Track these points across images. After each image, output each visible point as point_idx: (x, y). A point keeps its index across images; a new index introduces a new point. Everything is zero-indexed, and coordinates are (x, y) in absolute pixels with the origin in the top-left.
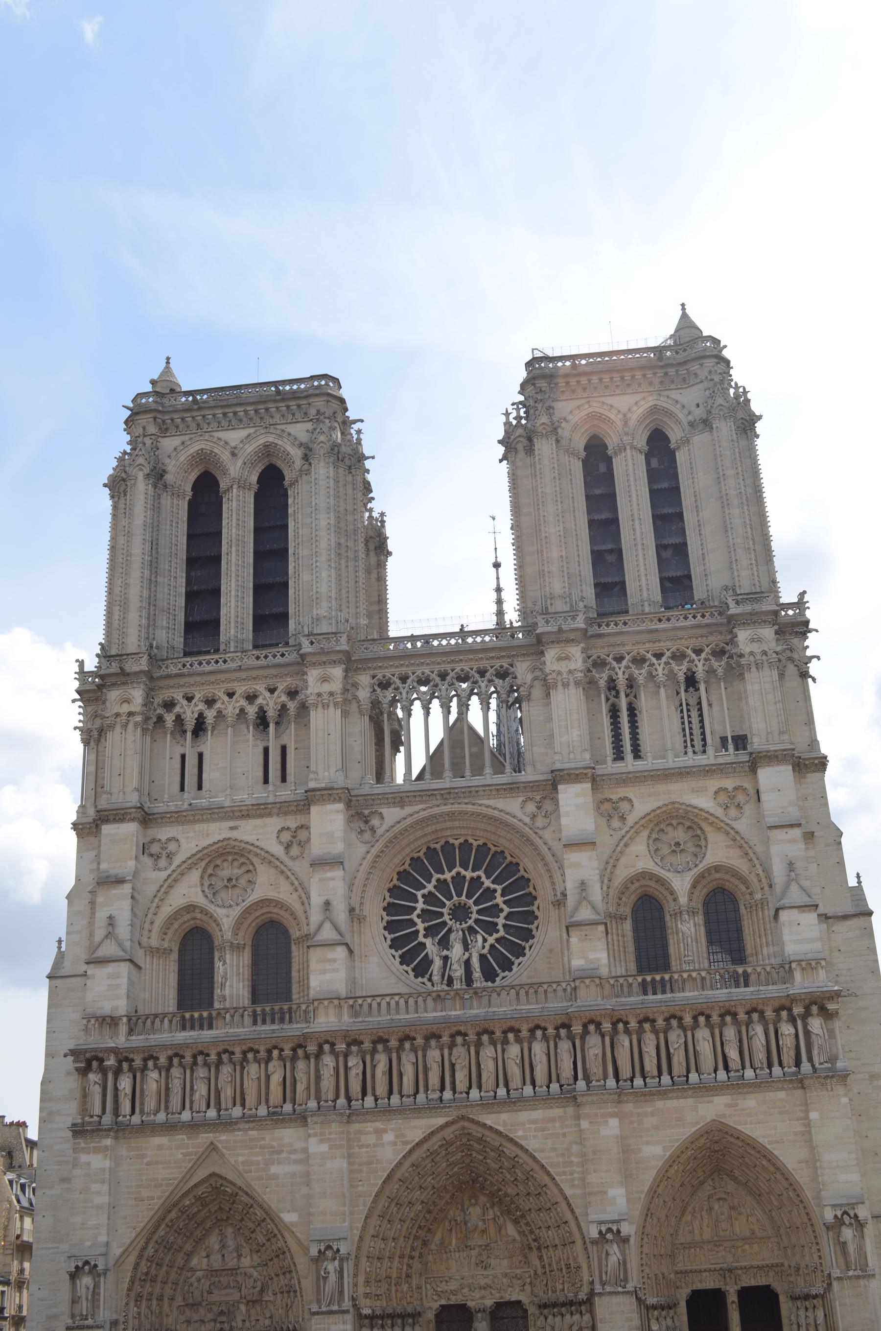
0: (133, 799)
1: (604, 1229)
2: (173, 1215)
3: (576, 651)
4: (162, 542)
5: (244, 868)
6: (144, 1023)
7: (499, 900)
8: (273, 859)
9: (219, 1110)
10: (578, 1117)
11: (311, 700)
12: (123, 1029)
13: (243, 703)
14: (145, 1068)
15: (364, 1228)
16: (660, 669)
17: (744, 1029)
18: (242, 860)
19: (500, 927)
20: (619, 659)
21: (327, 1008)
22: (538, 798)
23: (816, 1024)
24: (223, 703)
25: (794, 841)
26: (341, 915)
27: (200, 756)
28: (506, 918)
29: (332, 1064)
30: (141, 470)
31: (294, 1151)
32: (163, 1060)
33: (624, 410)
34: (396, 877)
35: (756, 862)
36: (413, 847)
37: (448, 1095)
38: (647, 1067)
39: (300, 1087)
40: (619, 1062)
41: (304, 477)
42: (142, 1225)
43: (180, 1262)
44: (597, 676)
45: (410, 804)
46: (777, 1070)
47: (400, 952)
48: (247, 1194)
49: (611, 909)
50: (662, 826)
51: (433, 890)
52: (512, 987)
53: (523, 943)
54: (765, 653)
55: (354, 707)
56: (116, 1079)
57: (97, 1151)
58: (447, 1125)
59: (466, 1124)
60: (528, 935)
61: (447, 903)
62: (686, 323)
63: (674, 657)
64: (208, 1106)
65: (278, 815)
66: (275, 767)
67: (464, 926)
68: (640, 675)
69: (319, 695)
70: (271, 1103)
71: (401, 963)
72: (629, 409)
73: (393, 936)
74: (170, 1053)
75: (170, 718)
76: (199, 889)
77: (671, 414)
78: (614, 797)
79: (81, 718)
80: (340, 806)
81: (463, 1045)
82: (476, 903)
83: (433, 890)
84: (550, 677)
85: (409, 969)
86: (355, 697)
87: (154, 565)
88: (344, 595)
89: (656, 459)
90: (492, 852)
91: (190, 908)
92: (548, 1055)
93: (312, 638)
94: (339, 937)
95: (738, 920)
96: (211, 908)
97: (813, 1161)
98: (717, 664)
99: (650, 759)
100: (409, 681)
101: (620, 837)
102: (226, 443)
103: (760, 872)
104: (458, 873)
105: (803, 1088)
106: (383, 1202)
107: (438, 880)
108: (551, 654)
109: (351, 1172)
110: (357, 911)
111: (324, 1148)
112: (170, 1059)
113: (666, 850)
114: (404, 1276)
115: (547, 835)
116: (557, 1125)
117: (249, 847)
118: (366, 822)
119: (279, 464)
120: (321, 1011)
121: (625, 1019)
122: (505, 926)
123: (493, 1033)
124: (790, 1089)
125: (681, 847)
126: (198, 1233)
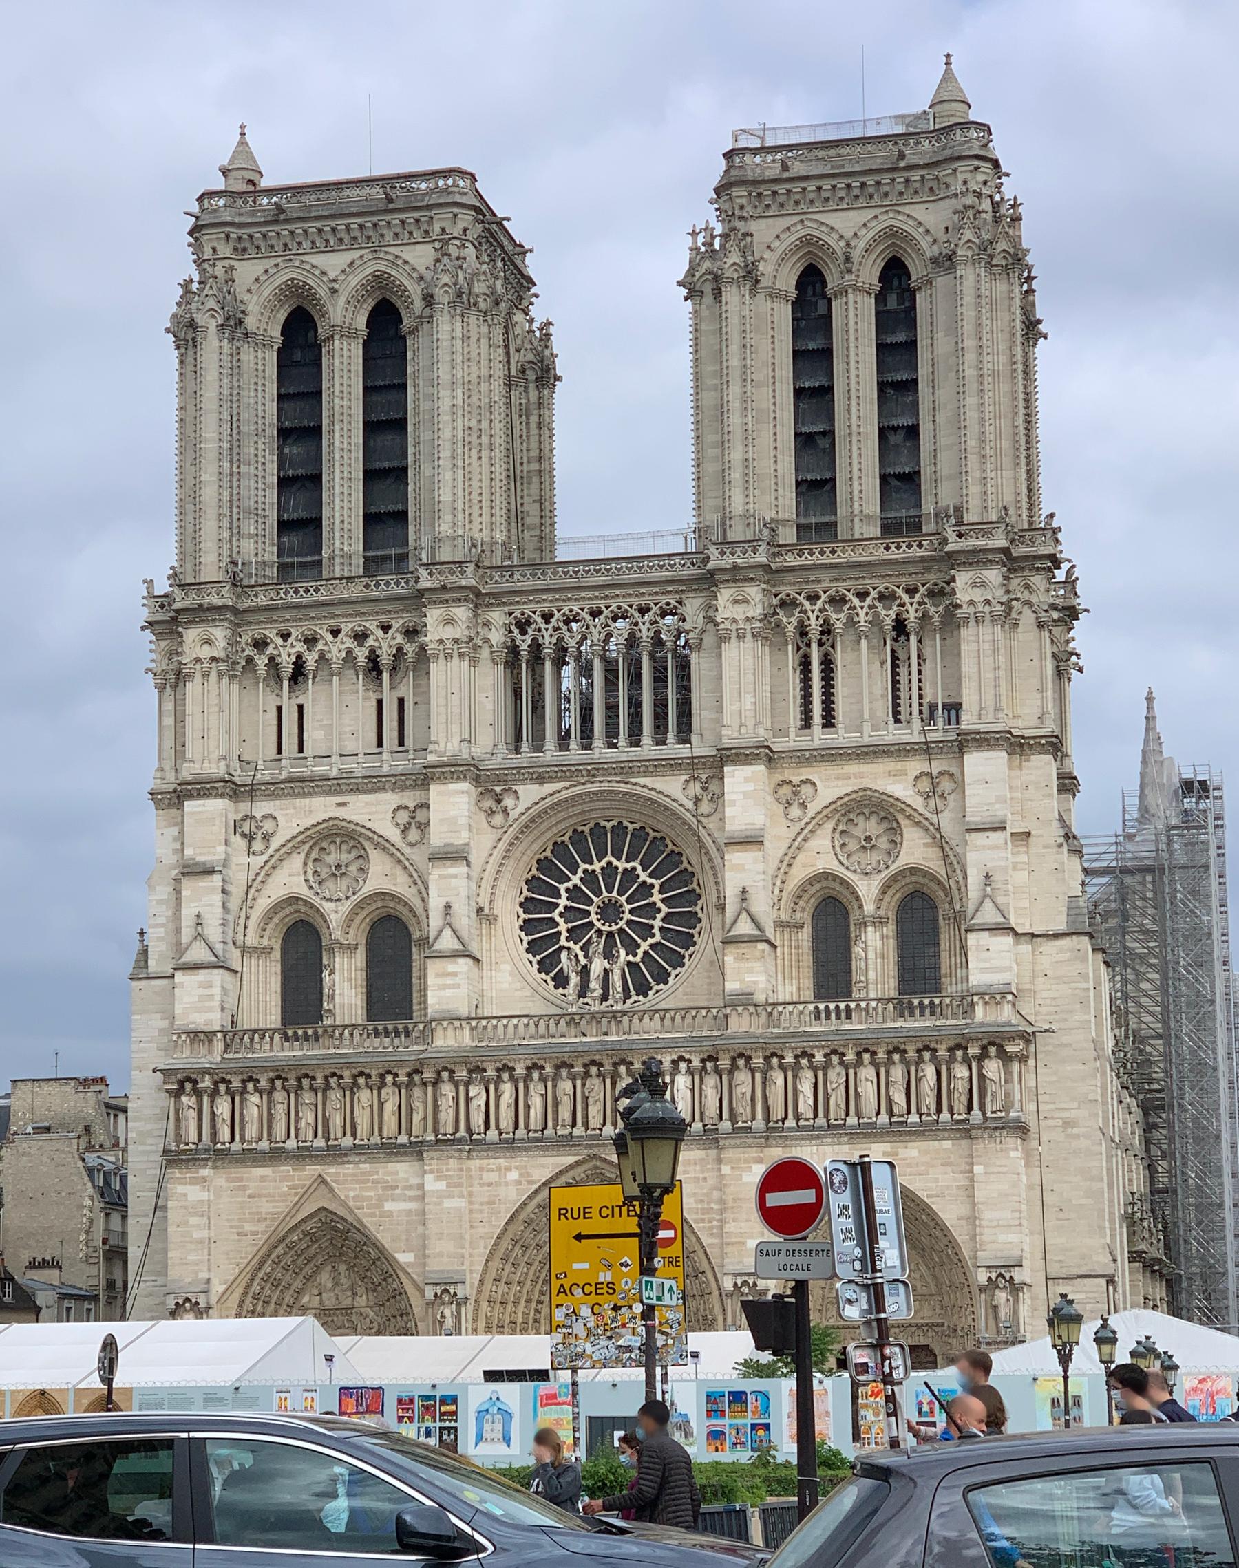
0: (220, 770)
1: (739, 1282)
2: (280, 1250)
3: (754, 592)
4: (244, 415)
5: (354, 853)
6: (242, 1039)
7: (656, 897)
8: (387, 845)
9: (328, 1139)
10: (719, 1161)
11: (432, 647)
12: (219, 1046)
13: (350, 643)
14: (244, 1091)
15: (485, 1272)
16: (862, 613)
17: (913, 1069)
18: (352, 843)
19: (656, 931)
20: (813, 598)
21: (445, 1029)
22: (704, 777)
23: (992, 1068)
24: (326, 644)
25: (996, 847)
26: (464, 917)
27: (301, 708)
28: (663, 920)
29: (451, 1094)
30: (213, 316)
31: (410, 1187)
32: (264, 1083)
33: (848, 234)
34: (535, 866)
35: (956, 866)
36: (555, 830)
37: (579, 1131)
38: (801, 1109)
39: (417, 1118)
40: (770, 1102)
41: (426, 326)
42: (246, 1261)
43: (288, 1298)
44: (785, 620)
45: (551, 780)
46: (945, 1116)
47: (538, 957)
48: (359, 1230)
49: (782, 917)
50: (852, 816)
51: (579, 883)
52: (656, 1011)
53: (682, 951)
54: (988, 602)
55: (485, 653)
56: (212, 1102)
57: (193, 1181)
58: (578, 1163)
59: (598, 1163)
60: (688, 941)
61: (595, 899)
62: (949, 94)
63: (881, 597)
64: (316, 1136)
65: (393, 790)
66: (392, 725)
67: (614, 928)
68: (838, 619)
69: (441, 642)
70: (385, 1135)
71: (539, 971)
72: (855, 234)
73: (530, 938)
74: (272, 1075)
75: (261, 661)
76: (302, 878)
77: (909, 239)
78: (796, 780)
79: (153, 656)
80: (465, 786)
81: (598, 1076)
82: (628, 901)
83: (579, 883)
84: (722, 626)
85: (548, 978)
86: (486, 640)
87: (236, 450)
88: (475, 497)
89: (894, 296)
90: (650, 838)
91: (293, 900)
92: (692, 1090)
93: (433, 568)
94: (461, 947)
95: (936, 932)
96: (317, 901)
97: (972, 1219)
98: (933, 609)
99: (841, 732)
100: (553, 620)
101: (798, 829)
102: (324, 273)
103: (960, 879)
104: (609, 863)
105: (970, 1137)
106: (506, 1244)
107: (585, 871)
108: (725, 595)
109: (471, 1211)
110: (486, 911)
111: (442, 1185)
112: (272, 1081)
113: (853, 845)
114: (531, 1321)
115: (711, 823)
116: (698, 1168)
117: (359, 829)
118: (499, 801)
119: (394, 299)
120: (439, 1033)
121: (780, 1053)
122: (661, 929)
123: (632, 1064)
124: (957, 1139)
125: (873, 842)
126: (308, 1270)
